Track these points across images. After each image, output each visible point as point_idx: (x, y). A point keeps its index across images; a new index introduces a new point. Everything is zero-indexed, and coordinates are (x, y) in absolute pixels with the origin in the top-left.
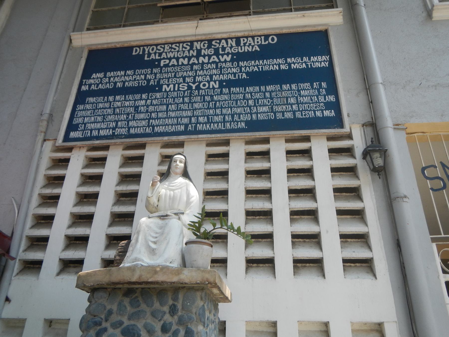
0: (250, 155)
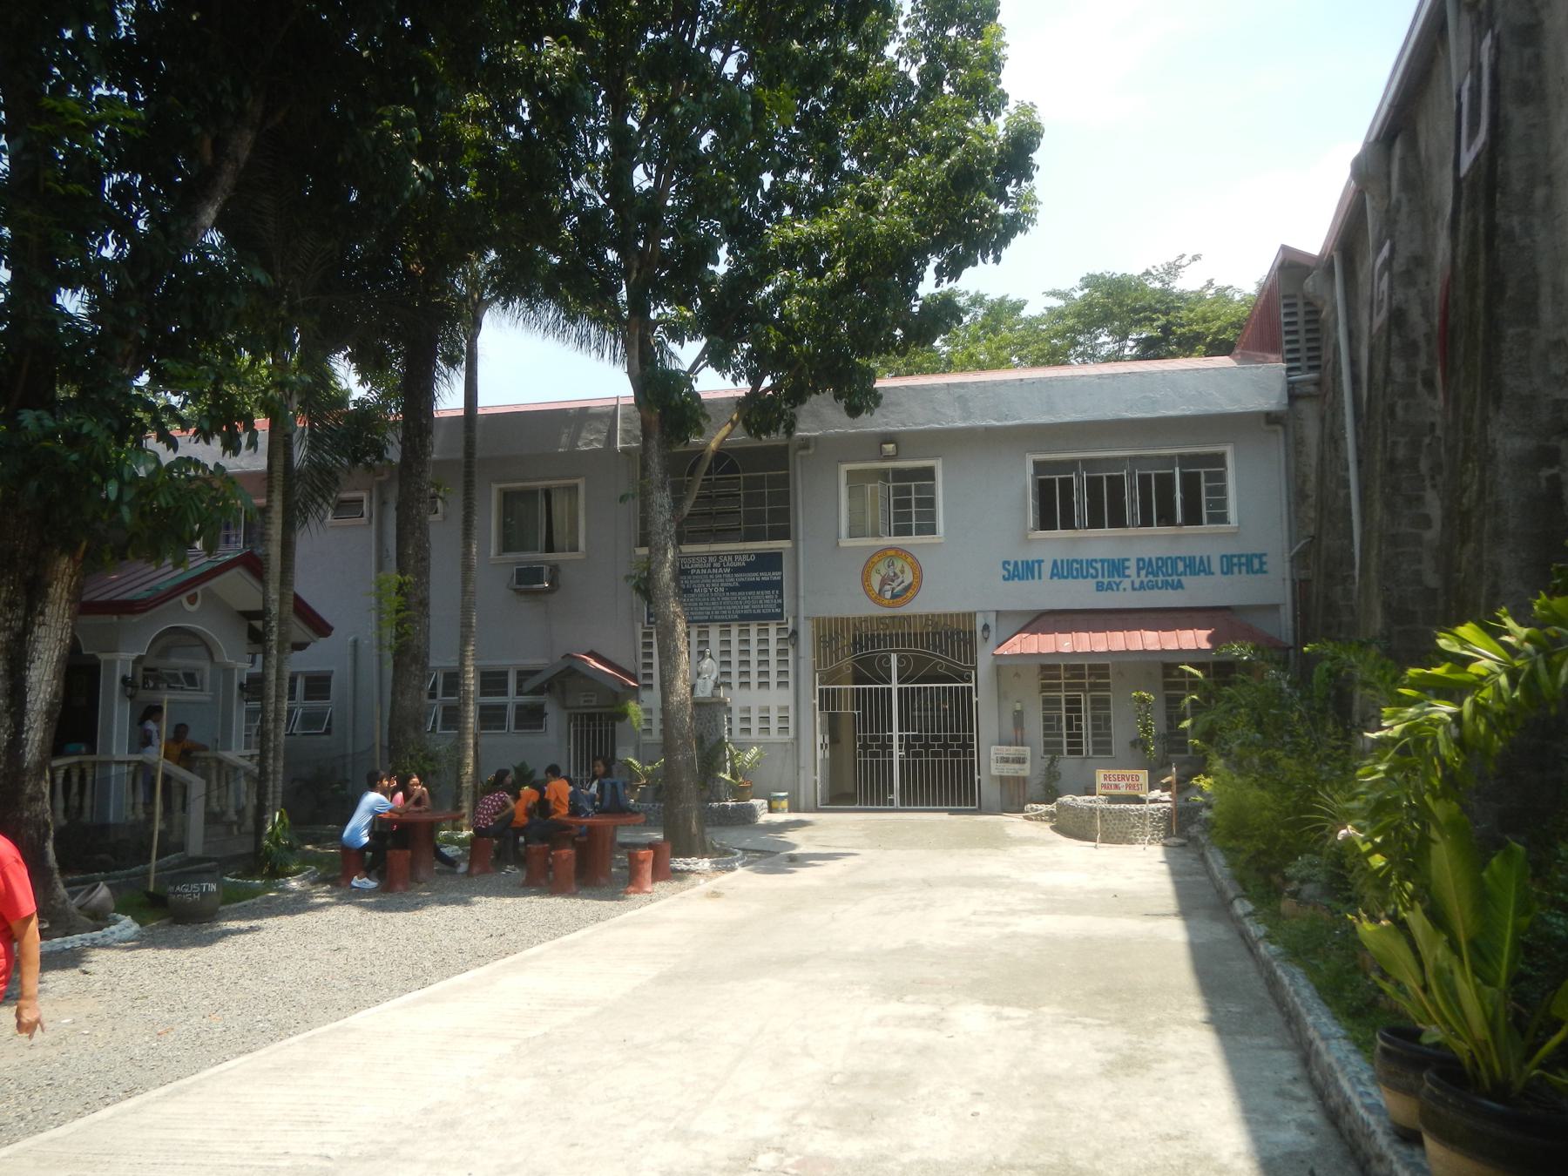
0: (741, 631)
